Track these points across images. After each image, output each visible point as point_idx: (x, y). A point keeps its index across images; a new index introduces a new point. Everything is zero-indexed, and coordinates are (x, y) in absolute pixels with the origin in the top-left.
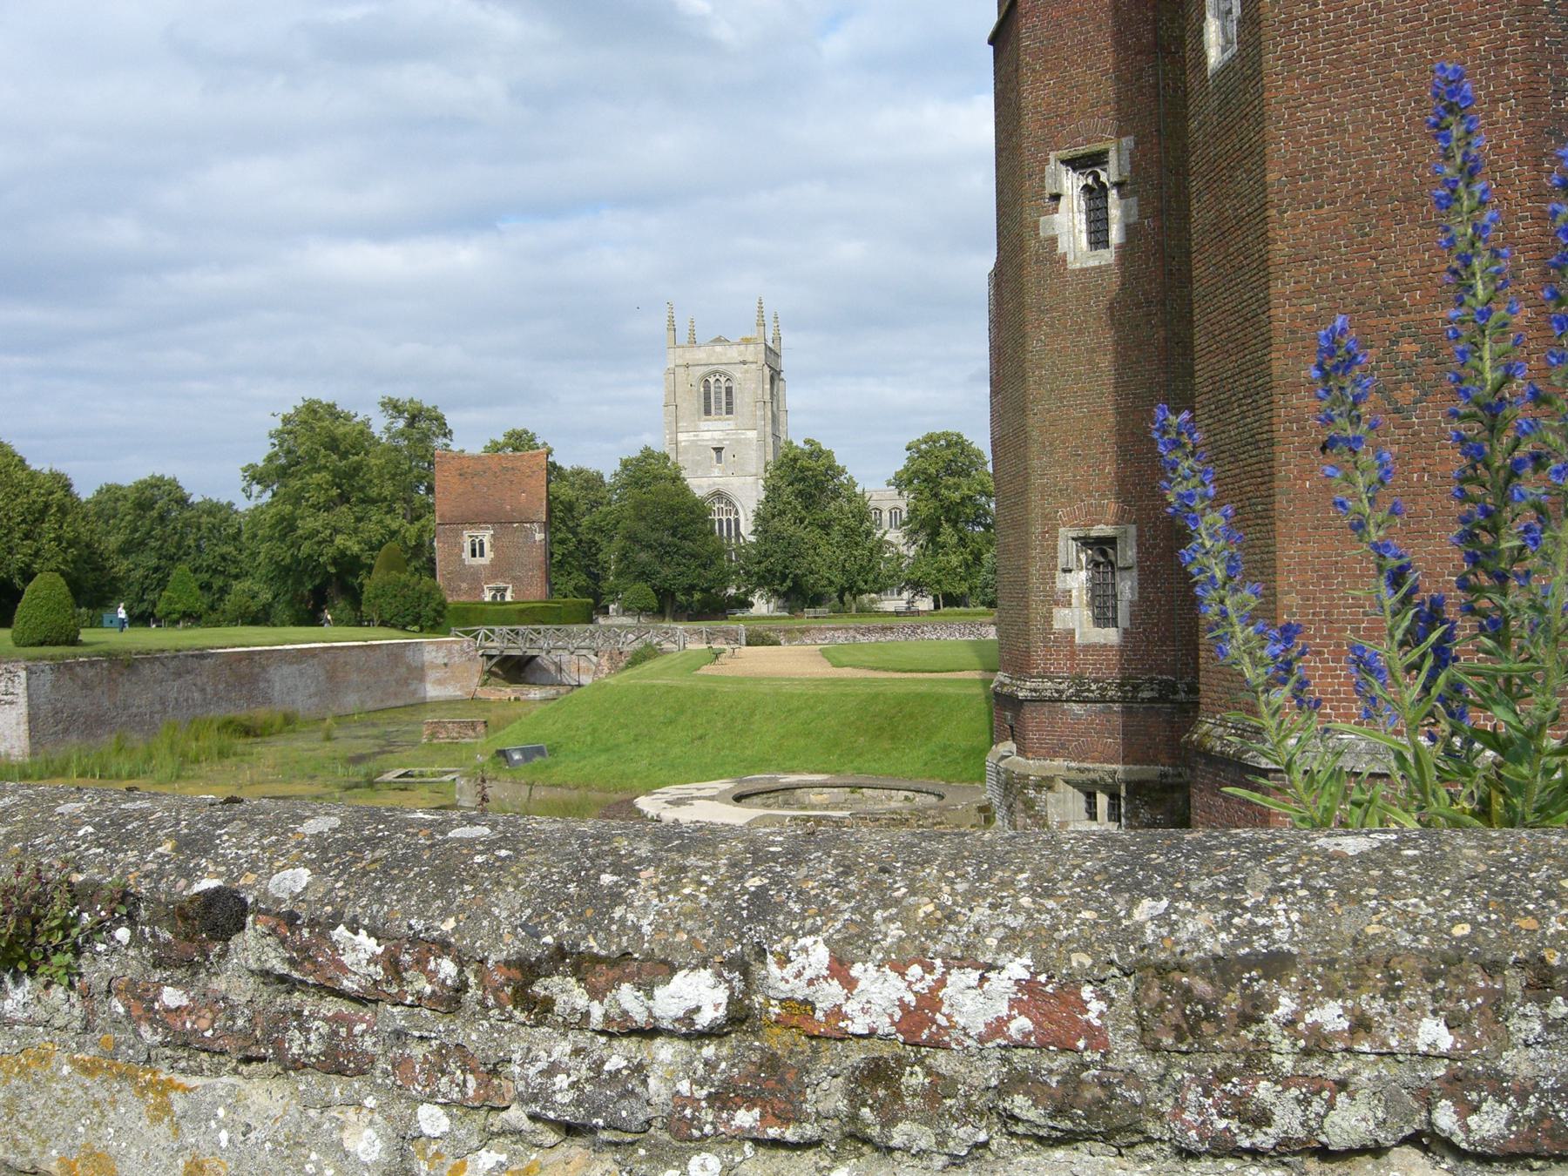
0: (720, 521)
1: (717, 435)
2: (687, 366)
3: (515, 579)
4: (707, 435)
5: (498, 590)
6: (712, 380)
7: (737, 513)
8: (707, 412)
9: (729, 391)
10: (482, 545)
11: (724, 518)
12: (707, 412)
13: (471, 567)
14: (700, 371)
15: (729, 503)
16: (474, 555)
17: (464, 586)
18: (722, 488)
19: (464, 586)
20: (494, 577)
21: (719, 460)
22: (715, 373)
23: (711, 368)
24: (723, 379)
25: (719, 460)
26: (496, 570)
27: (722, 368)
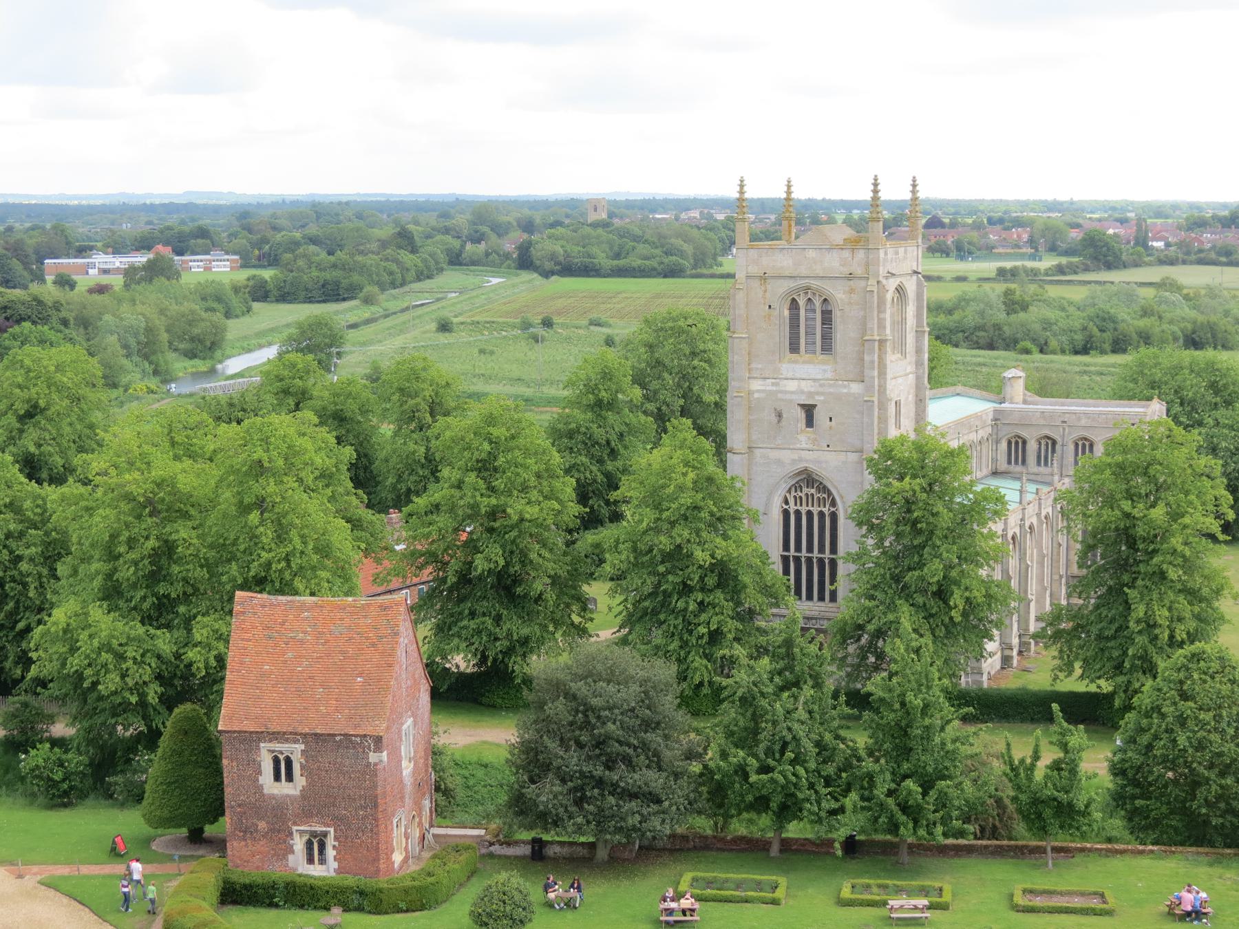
0: (810, 514)
1: (806, 386)
2: (764, 278)
3: (338, 821)
4: (792, 386)
5: (314, 834)
6: (802, 302)
7: (833, 503)
8: (794, 348)
9: (827, 317)
10: (289, 762)
11: (815, 510)
12: (794, 348)
13: (273, 797)
14: (784, 286)
15: (823, 489)
16: (277, 778)
17: (262, 825)
18: (811, 466)
19: (262, 825)
20: (306, 814)
21: (810, 422)
22: (807, 289)
24: (817, 303)
25: (810, 422)
26: (310, 806)
27: (814, 283)
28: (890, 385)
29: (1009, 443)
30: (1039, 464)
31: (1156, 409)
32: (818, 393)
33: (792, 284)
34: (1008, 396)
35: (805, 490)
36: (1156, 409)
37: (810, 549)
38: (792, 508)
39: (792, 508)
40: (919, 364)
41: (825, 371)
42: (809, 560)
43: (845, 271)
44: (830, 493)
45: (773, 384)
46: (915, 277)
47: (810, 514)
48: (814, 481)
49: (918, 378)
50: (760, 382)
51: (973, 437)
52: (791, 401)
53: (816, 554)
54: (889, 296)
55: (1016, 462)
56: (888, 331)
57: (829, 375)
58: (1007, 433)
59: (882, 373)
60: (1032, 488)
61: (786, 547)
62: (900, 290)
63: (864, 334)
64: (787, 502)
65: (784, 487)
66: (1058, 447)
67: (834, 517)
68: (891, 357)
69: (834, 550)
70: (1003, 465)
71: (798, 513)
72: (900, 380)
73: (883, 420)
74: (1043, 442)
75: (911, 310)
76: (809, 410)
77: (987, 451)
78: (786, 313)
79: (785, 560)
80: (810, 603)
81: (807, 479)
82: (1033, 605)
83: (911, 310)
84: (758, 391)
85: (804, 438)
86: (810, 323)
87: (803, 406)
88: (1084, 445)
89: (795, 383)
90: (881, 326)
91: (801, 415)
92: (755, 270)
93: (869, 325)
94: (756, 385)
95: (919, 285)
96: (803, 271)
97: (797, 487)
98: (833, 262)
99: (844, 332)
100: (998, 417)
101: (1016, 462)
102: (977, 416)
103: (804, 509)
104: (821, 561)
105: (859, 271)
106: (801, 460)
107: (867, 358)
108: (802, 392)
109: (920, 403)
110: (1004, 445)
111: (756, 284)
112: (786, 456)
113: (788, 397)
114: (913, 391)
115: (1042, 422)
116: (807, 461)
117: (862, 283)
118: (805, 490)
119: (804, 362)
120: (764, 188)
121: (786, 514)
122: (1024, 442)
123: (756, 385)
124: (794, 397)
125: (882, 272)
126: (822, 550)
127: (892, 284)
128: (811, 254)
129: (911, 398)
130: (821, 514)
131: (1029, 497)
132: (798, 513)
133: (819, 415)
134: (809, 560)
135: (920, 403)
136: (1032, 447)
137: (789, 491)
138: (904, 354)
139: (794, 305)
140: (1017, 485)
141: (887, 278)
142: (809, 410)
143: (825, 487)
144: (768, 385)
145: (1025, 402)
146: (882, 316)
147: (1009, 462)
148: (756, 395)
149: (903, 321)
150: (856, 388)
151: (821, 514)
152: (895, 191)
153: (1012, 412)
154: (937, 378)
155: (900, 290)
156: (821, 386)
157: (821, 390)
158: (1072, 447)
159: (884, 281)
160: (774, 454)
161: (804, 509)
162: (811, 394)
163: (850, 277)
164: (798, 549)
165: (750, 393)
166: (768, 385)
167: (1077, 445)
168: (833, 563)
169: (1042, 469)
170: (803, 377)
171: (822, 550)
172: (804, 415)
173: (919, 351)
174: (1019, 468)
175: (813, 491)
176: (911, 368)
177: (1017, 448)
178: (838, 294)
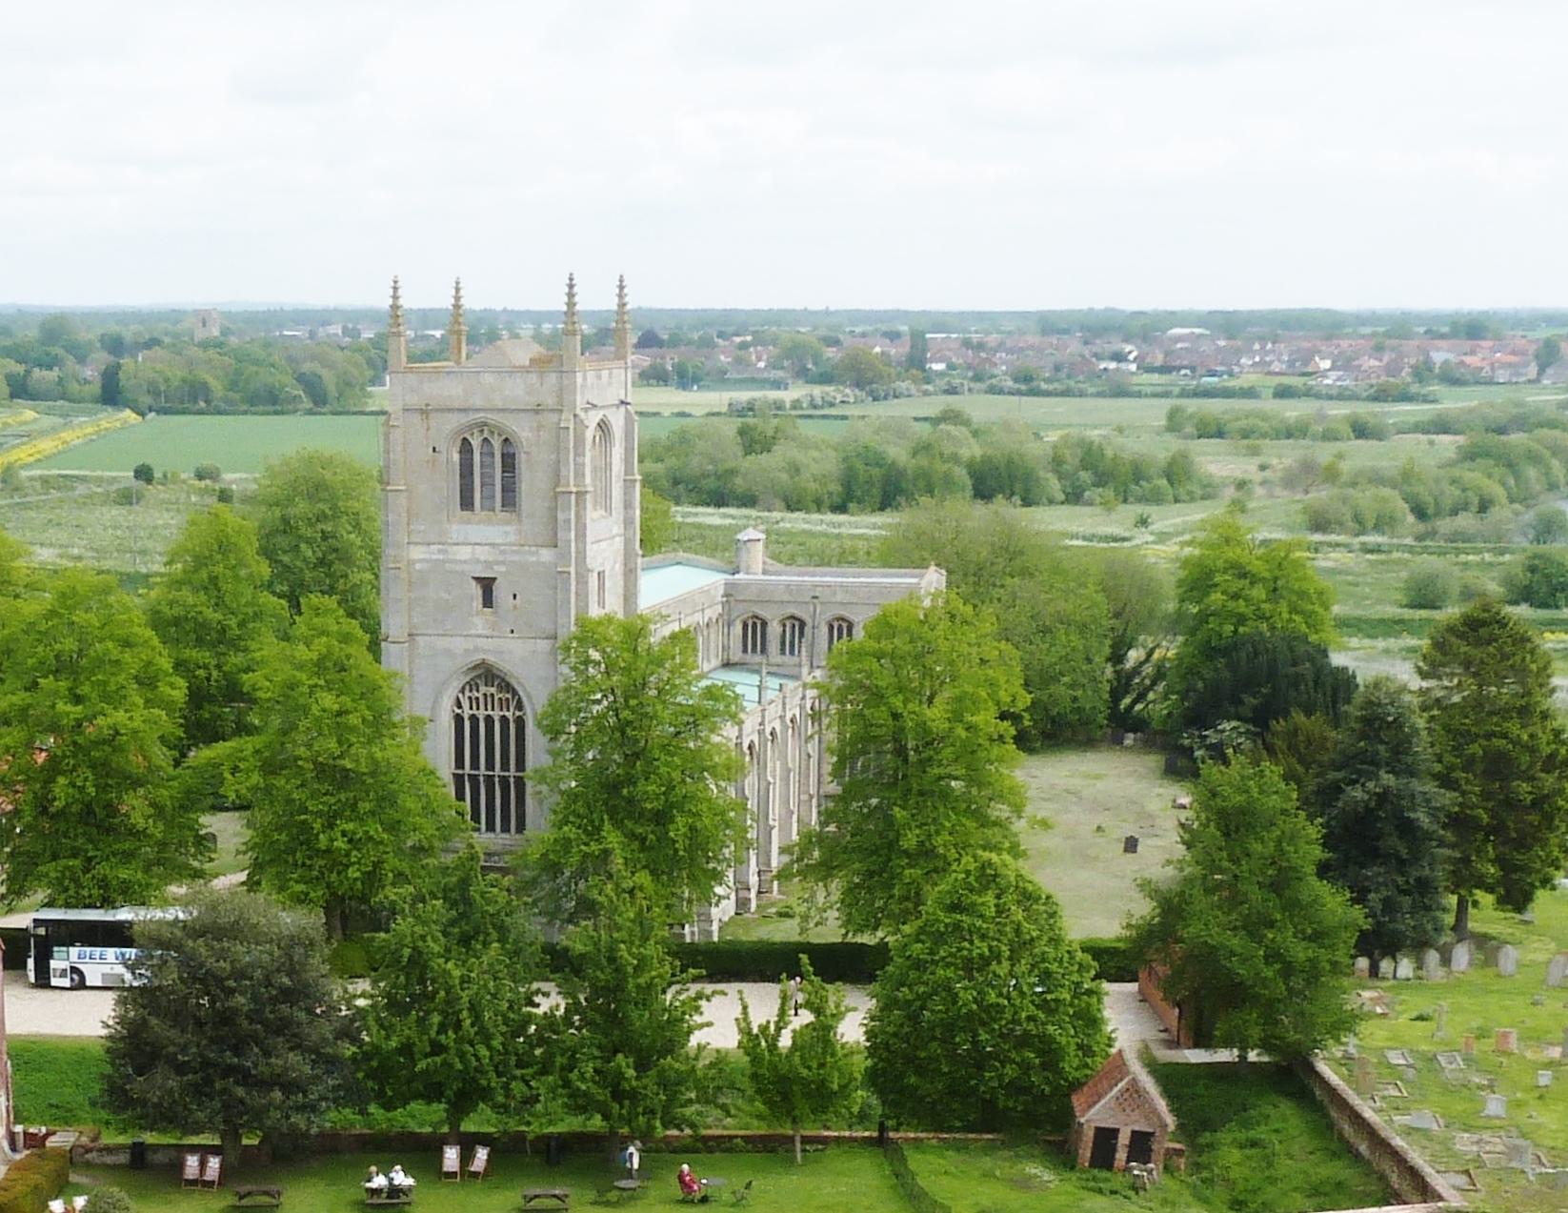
0: (489, 720)
1: (483, 553)
2: (424, 412)
4: (464, 553)
7: (520, 706)
8: (467, 503)
9: (509, 462)
11: (496, 714)
15: (506, 686)
18: (491, 659)
21: (488, 601)
22: (482, 426)
23: (472, 417)
24: (497, 444)
25: (488, 601)
27: (492, 418)
28: (591, 550)
29: (745, 626)
30: (783, 651)
31: (933, 579)
32: (498, 563)
33: (465, 419)
34: (743, 566)
35: (483, 689)
36: (933, 579)
37: (490, 766)
38: (467, 713)
39: (467, 713)
40: (628, 522)
41: (506, 533)
42: (489, 779)
43: (531, 401)
44: (515, 693)
45: (439, 551)
46: (622, 409)
47: (489, 720)
48: (494, 676)
49: (628, 543)
50: (423, 549)
51: (698, 617)
52: (463, 573)
53: (498, 771)
54: (589, 434)
55: (754, 650)
56: (588, 480)
57: (512, 538)
58: (741, 612)
59: (581, 535)
60: (773, 683)
61: (459, 762)
62: (603, 426)
63: (557, 485)
64: (460, 706)
65: (456, 684)
66: (807, 630)
67: (520, 723)
68: (593, 515)
69: (521, 764)
70: (736, 655)
71: (474, 719)
72: (603, 545)
73: (583, 596)
74: (788, 624)
75: (618, 452)
76: (487, 585)
77: (716, 638)
78: (456, 457)
79: (459, 780)
80: (491, 835)
81: (486, 674)
82: (775, 833)
83: (618, 452)
84: (420, 561)
85: (480, 621)
86: (489, 470)
87: (476, 579)
88: (841, 627)
89: (469, 549)
90: (580, 474)
91: (477, 591)
92: (413, 400)
93: (563, 473)
94: (417, 553)
95: (628, 418)
96: (478, 403)
97: (472, 685)
98: (517, 390)
99: (531, 482)
100: (730, 593)
101: (754, 650)
102: (704, 592)
103: (481, 714)
104: (504, 781)
105: (550, 401)
106: (476, 650)
107: (560, 516)
108: (478, 561)
109: (630, 574)
110: (738, 629)
111: (416, 418)
112: (459, 645)
113: (458, 568)
114: (620, 558)
115: (786, 598)
116: (484, 651)
117: (554, 417)
118: (483, 689)
119: (479, 522)
120: (425, 295)
121: (459, 720)
122: (764, 624)
123: (417, 553)
124: (466, 567)
125: (580, 402)
126: (505, 766)
127: (593, 419)
128: (488, 379)
129: (619, 568)
130: (504, 720)
131: (770, 695)
132: (474, 719)
133: (500, 592)
134: (489, 779)
135: (630, 574)
136: (774, 629)
137: (462, 691)
138: (608, 509)
139: (466, 447)
140: (755, 679)
141: (586, 410)
142: (487, 585)
143: (508, 685)
144: (432, 553)
145: (765, 572)
146: (579, 460)
147: (745, 651)
148: (418, 566)
149: (608, 466)
150: (546, 555)
151: (504, 720)
152: (596, 299)
153: (748, 585)
154: (653, 541)
155: (603, 426)
156: (503, 552)
157: (501, 558)
158: (825, 629)
159: (582, 415)
160: (443, 643)
161: (481, 714)
162: (488, 564)
163: (537, 410)
164: (475, 765)
165: (411, 563)
166: (432, 553)
167: (831, 627)
168: (520, 783)
169: (787, 658)
170: (481, 540)
171: (505, 766)
172: (480, 592)
173: (628, 505)
174: (758, 658)
175: (493, 690)
176: (617, 529)
177: (755, 632)
178: (523, 431)
